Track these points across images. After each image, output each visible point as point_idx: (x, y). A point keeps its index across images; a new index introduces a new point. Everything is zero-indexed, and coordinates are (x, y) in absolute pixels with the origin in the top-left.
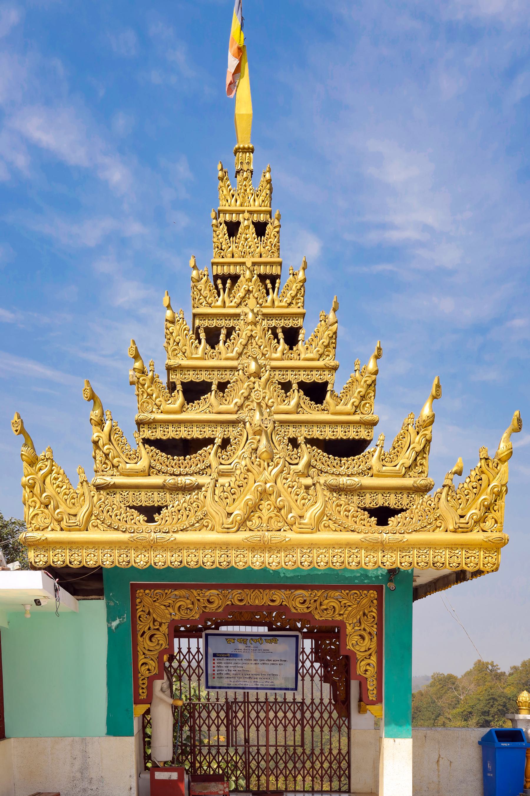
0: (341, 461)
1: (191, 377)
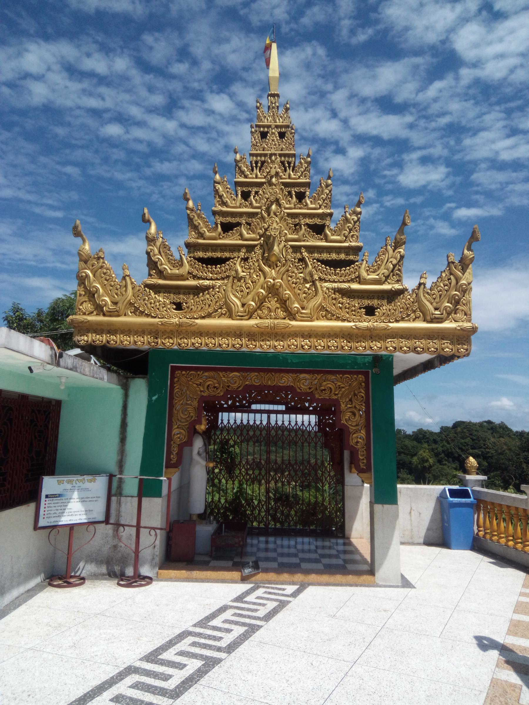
0: (335, 271)
1: (229, 219)
